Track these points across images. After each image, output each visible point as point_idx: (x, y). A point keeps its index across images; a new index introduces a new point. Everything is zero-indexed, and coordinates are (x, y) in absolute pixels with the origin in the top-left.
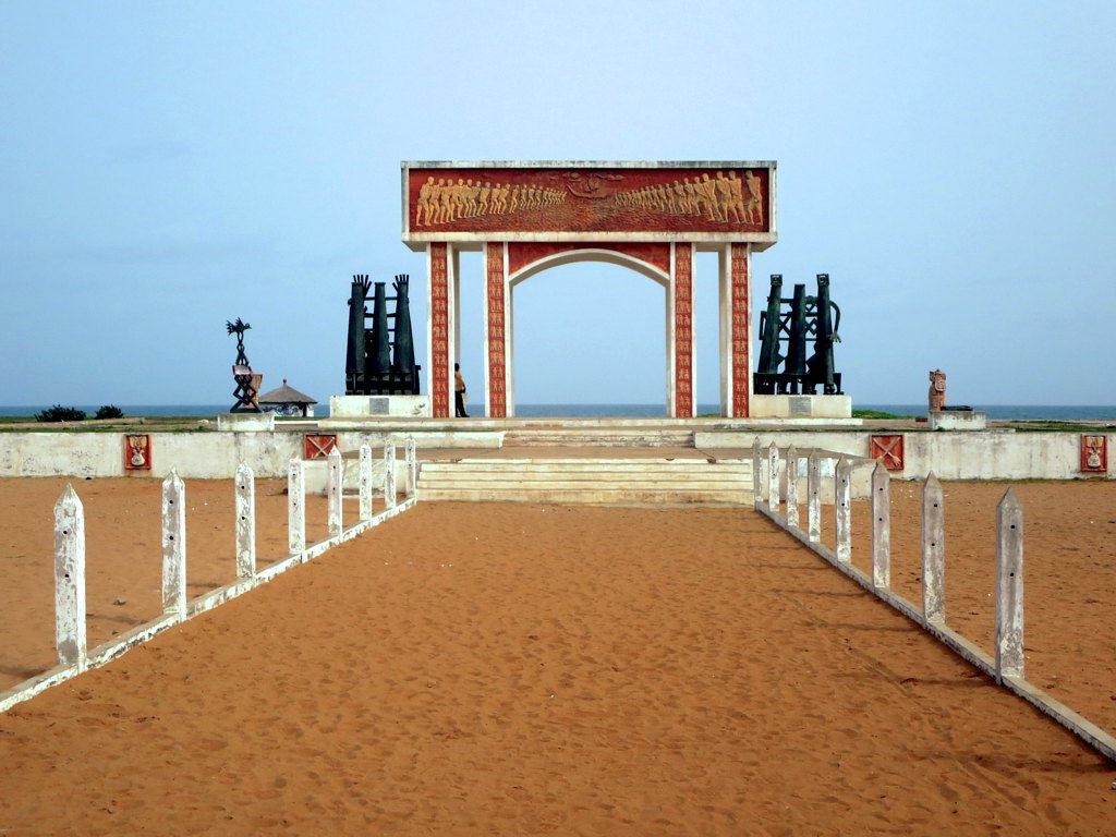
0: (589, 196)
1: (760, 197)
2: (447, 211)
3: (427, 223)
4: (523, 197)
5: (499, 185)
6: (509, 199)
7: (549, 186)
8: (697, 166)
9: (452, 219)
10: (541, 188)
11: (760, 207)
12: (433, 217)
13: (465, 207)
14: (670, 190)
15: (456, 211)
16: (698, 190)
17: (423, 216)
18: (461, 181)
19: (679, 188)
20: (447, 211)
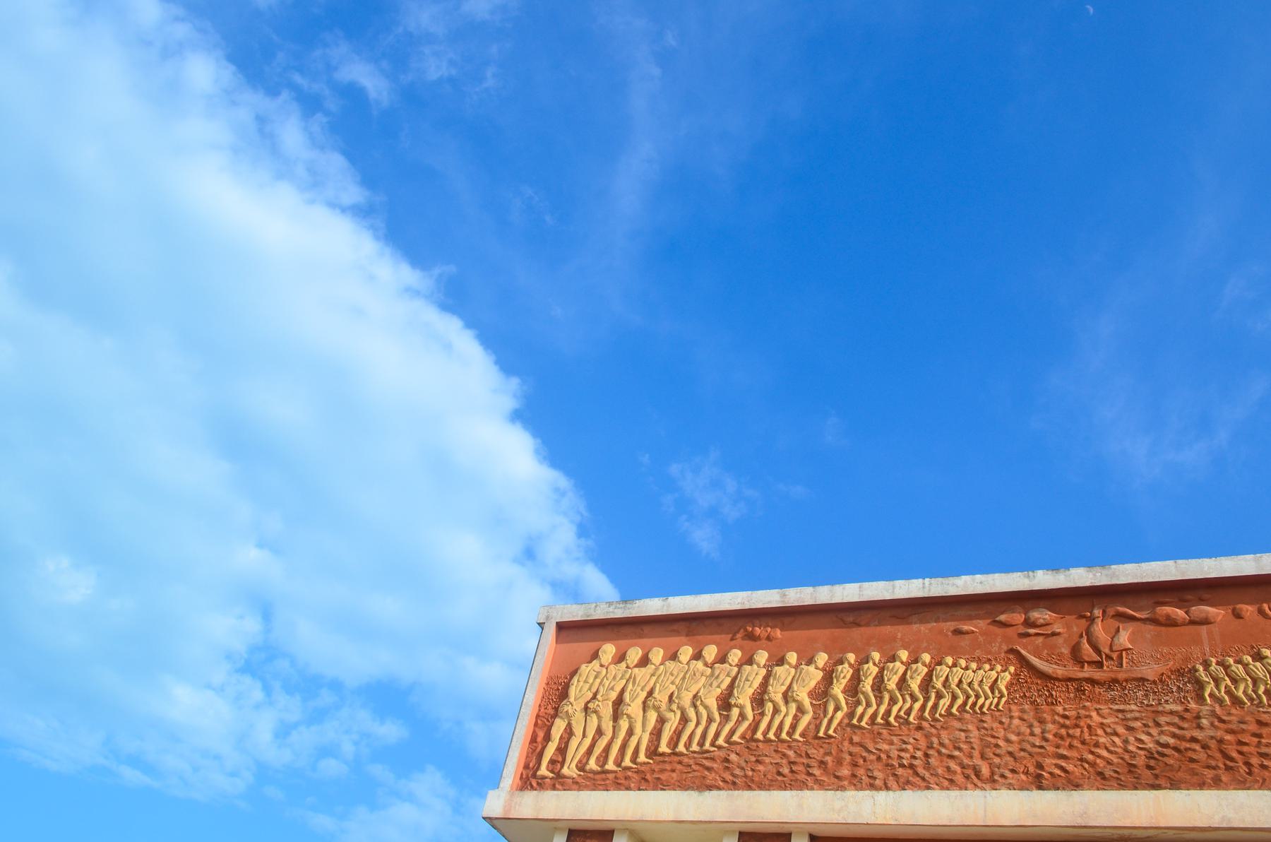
0: (1097, 675)
2: (630, 732)
3: (570, 770)
4: (867, 685)
5: (792, 657)
6: (822, 694)
7: (956, 652)
9: (642, 758)
10: (926, 657)
13: (684, 720)
15: (657, 734)
17: (562, 750)
18: (686, 652)
20: (630, 732)
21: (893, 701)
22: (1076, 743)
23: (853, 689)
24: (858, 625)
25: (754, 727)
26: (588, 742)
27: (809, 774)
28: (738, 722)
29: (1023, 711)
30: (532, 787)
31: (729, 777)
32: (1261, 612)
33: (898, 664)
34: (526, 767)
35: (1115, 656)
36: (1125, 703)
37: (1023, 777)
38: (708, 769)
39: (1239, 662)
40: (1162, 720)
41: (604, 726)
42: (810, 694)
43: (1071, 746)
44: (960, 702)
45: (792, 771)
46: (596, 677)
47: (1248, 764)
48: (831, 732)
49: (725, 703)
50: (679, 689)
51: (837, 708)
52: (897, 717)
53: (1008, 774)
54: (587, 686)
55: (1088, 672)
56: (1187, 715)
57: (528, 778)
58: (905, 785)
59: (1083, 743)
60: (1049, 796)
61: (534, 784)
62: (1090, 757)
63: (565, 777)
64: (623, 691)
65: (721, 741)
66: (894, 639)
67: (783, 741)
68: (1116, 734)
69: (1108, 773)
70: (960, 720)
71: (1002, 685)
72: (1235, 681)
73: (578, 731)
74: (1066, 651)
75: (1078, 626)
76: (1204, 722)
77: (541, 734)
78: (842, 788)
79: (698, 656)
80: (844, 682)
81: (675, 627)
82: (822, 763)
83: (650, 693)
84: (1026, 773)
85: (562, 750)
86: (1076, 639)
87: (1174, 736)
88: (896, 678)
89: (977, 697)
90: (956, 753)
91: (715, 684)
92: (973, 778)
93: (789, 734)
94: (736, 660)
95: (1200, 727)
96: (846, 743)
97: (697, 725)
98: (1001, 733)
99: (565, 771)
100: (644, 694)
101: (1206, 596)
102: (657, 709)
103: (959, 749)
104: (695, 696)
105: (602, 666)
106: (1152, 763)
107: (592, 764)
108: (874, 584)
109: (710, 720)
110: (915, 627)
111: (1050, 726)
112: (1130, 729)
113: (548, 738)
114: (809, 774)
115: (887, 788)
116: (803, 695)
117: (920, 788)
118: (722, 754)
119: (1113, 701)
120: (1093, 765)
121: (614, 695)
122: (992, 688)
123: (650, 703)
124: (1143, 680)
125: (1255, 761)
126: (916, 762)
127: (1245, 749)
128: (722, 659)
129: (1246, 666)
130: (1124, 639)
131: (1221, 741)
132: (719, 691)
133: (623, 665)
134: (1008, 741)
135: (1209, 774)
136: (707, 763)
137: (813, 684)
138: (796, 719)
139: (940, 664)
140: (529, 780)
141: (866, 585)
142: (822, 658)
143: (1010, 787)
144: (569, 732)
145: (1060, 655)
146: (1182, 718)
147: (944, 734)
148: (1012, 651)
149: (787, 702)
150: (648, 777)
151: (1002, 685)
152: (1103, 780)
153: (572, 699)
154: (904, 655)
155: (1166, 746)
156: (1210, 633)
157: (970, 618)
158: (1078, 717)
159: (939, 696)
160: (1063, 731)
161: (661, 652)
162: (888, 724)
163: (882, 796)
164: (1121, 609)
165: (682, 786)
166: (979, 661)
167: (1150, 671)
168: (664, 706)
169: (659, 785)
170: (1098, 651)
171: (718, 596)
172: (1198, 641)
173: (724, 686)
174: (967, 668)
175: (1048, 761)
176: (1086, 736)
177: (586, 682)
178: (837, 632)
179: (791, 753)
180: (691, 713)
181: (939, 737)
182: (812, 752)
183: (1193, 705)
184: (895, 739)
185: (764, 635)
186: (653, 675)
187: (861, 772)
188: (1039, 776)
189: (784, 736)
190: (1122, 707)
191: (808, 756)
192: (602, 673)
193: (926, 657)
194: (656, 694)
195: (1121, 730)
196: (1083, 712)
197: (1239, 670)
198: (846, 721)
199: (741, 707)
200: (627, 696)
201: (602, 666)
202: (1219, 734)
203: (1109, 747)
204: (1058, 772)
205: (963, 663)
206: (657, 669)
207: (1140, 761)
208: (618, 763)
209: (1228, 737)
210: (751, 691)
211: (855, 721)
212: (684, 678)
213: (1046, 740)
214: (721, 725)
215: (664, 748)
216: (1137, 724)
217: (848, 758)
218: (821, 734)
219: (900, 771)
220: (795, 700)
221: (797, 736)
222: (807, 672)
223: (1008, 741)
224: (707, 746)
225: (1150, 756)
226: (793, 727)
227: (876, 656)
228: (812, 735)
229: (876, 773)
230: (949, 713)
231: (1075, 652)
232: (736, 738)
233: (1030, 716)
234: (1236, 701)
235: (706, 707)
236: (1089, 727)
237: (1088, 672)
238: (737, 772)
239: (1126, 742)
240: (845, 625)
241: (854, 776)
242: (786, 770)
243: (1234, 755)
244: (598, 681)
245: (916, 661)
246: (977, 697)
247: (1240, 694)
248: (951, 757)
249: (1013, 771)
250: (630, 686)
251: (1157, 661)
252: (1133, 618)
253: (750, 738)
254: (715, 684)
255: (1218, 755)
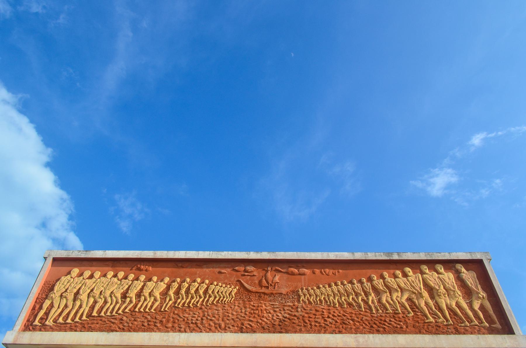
0: (267, 291)
1: (483, 294)
2: (80, 307)
3: (49, 322)
4: (183, 291)
6: (165, 294)
7: (218, 280)
8: (395, 257)
9: (84, 318)
10: (207, 281)
11: (488, 305)
12: (60, 315)
13: (106, 302)
14: (368, 285)
15: (92, 308)
16: (402, 285)
17: (47, 314)
18: (110, 274)
19: (379, 283)
20: (80, 307)
21: (192, 298)
22: (256, 316)
23: (177, 292)
24: (182, 267)
25: (135, 306)
26: (60, 310)
27: (155, 326)
28: (129, 304)
29: (239, 303)
30: (30, 330)
31: (121, 326)
32: (321, 272)
33: (196, 283)
34: (28, 321)
35: (273, 285)
36: (275, 302)
37: (236, 328)
38: (113, 323)
39: (312, 289)
40: (286, 308)
41: (68, 304)
42: (160, 294)
43: (254, 317)
44: (217, 299)
45: (148, 324)
46: (68, 282)
47: (311, 325)
48: (166, 309)
49: (124, 296)
50: (105, 289)
51: (170, 300)
52: (193, 304)
53: (231, 327)
54: (64, 286)
55: (264, 290)
56: (294, 307)
57: (28, 326)
58: (192, 331)
59: (259, 316)
60: (244, 335)
61: (31, 329)
62: (260, 321)
63: (46, 325)
64: (80, 289)
65: (120, 312)
66: (196, 274)
67: (146, 312)
68: (270, 313)
69: (266, 327)
70: (216, 306)
71: (233, 294)
72: (310, 295)
73: (56, 305)
74: (257, 282)
75: (262, 273)
76: (299, 309)
77: (38, 306)
78: (168, 332)
79: (115, 276)
80: (174, 289)
81: (107, 263)
82: (161, 321)
83: (92, 290)
84: (237, 327)
85: (47, 314)
86: (261, 278)
87: (289, 314)
88: (194, 289)
89: (224, 297)
90: (213, 319)
91: (121, 288)
92: (219, 328)
93: (150, 309)
94: (132, 278)
95: (297, 311)
96: (172, 314)
97: (111, 305)
98: (230, 312)
99: (47, 323)
100: (89, 291)
101: (305, 265)
102: (94, 297)
103: (215, 317)
104: (112, 292)
105: (71, 277)
106: (281, 324)
107: (61, 320)
108: (191, 252)
109: (117, 303)
110: (204, 270)
111: (248, 309)
112: (275, 311)
113: (41, 308)
114: (155, 326)
115: (185, 332)
116: (157, 294)
117: (198, 332)
118: (120, 317)
119: (270, 301)
120: (261, 324)
121: (75, 290)
122: (229, 295)
123: (91, 295)
124: (281, 294)
125: (313, 324)
126: (198, 322)
127: (311, 319)
128: (126, 278)
129: (314, 290)
130: (277, 279)
131: (303, 316)
132: (122, 291)
133: (82, 278)
134: (232, 314)
135: (298, 328)
136: (113, 321)
137: (162, 289)
138: (153, 303)
139: (212, 284)
140: (29, 326)
141: (188, 252)
142: (167, 280)
143: (231, 332)
144: (52, 306)
145: (255, 283)
146: (292, 308)
147: (210, 311)
148: (238, 281)
149: (150, 296)
150: (86, 326)
151: (233, 294)
152: (264, 330)
153: (55, 291)
154: (199, 280)
155: (286, 318)
156: (305, 279)
157: (225, 268)
158: (258, 306)
159: (210, 297)
160: (252, 311)
161: (100, 273)
162: (189, 306)
163: (183, 335)
164: (277, 268)
165: (101, 330)
166: (226, 284)
167: (284, 291)
168: (97, 296)
169: (91, 329)
170: (268, 283)
171: (127, 252)
172: (300, 281)
173: (125, 289)
174: (221, 286)
175: (246, 322)
176: (260, 313)
177: (63, 284)
178: (174, 269)
179: (149, 317)
180: (109, 300)
181: (208, 312)
182: (158, 317)
183: (296, 303)
184: (191, 313)
185: (145, 269)
186: (94, 283)
187: (176, 325)
188: (242, 328)
189: (147, 310)
190: (273, 303)
191: (156, 318)
192: (71, 281)
193: (207, 281)
194: (94, 291)
195: (272, 311)
196: (260, 304)
197: (312, 292)
198: (173, 305)
199: (131, 298)
200: (81, 291)
201: (71, 277)
202: (303, 314)
203: (267, 318)
204: (248, 326)
205: (220, 284)
206: (96, 280)
207: (277, 323)
208: (73, 320)
209: (306, 315)
210: (136, 291)
211: (176, 305)
212: (108, 284)
213: (246, 314)
214: (121, 305)
215: (95, 314)
216: (277, 310)
217: (172, 319)
218: (162, 310)
219: (191, 325)
220: (153, 296)
221: (152, 310)
222: (160, 285)
223: (232, 314)
224: (114, 313)
225: (280, 321)
226: (151, 307)
227: (188, 280)
228: (159, 310)
229: (182, 326)
230: (213, 303)
231: (260, 282)
232: (127, 310)
233: (241, 305)
234: (310, 303)
235: (116, 297)
236: (261, 310)
237: (264, 290)
238: (126, 324)
239: (273, 316)
240: (178, 267)
241: (173, 327)
242: (146, 324)
243: (307, 321)
244: (69, 284)
245: (203, 283)
246: (224, 297)
247: (311, 300)
248: (211, 320)
249: (233, 326)
250: (83, 287)
251: (287, 287)
252: (281, 272)
253: (133, 311)
254: (121, 288)
255: (302, 321)
